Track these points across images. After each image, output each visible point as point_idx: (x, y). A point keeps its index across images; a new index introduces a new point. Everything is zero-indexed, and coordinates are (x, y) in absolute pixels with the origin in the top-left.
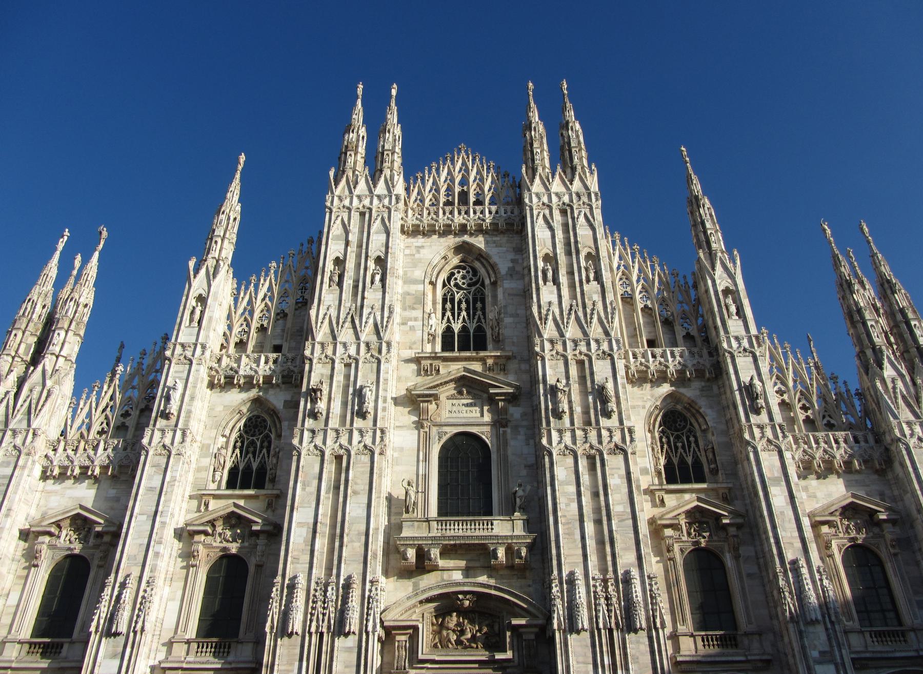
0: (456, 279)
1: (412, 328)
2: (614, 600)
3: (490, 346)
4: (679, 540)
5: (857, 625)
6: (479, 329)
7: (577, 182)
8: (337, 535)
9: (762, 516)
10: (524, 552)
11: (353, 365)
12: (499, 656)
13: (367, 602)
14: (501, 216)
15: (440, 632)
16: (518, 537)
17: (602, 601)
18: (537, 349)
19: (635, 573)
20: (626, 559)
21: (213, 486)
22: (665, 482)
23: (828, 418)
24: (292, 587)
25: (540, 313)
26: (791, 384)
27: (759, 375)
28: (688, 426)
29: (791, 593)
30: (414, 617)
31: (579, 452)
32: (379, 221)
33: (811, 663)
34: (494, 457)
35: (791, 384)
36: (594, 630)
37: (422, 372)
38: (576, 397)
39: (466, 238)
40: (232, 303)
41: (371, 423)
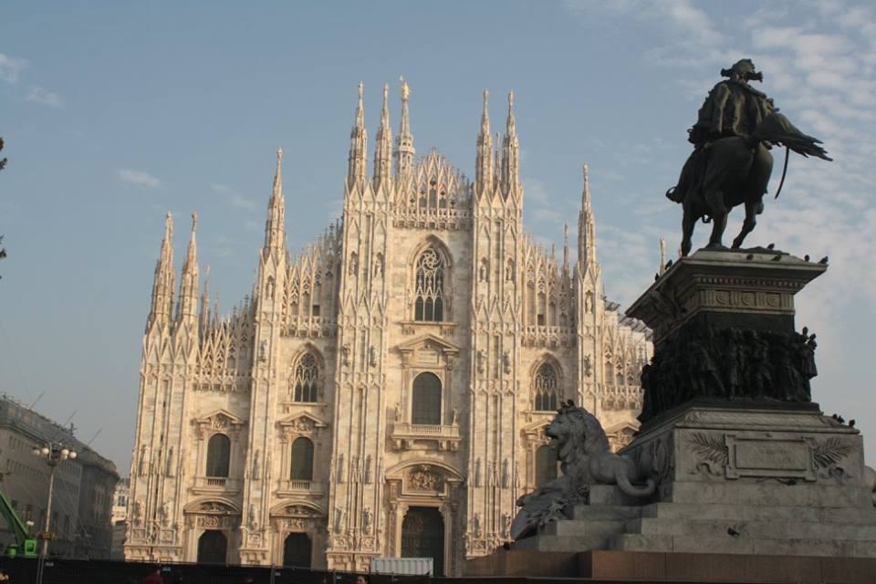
1: (398, 300)
2: (498, 473)
3: (445, 314)
7: (509, 200)
8: (362, 433)
10: (456, 445)
11: (367, 332)
12: (440, 495)
13: (378, 468)
18: (473, 328)
19: (510, 460)
20: (507, 452)
21: (288, 399)
24: (341, 460)
27: (595, 352)
30: (400, 476)
31: (489, 394)
32: (379, 225)
35: (615, 352)
36: (487, 486)
37: (405, 332)
38: (492, 359)
39: (434, 232)
41: (378, 370)
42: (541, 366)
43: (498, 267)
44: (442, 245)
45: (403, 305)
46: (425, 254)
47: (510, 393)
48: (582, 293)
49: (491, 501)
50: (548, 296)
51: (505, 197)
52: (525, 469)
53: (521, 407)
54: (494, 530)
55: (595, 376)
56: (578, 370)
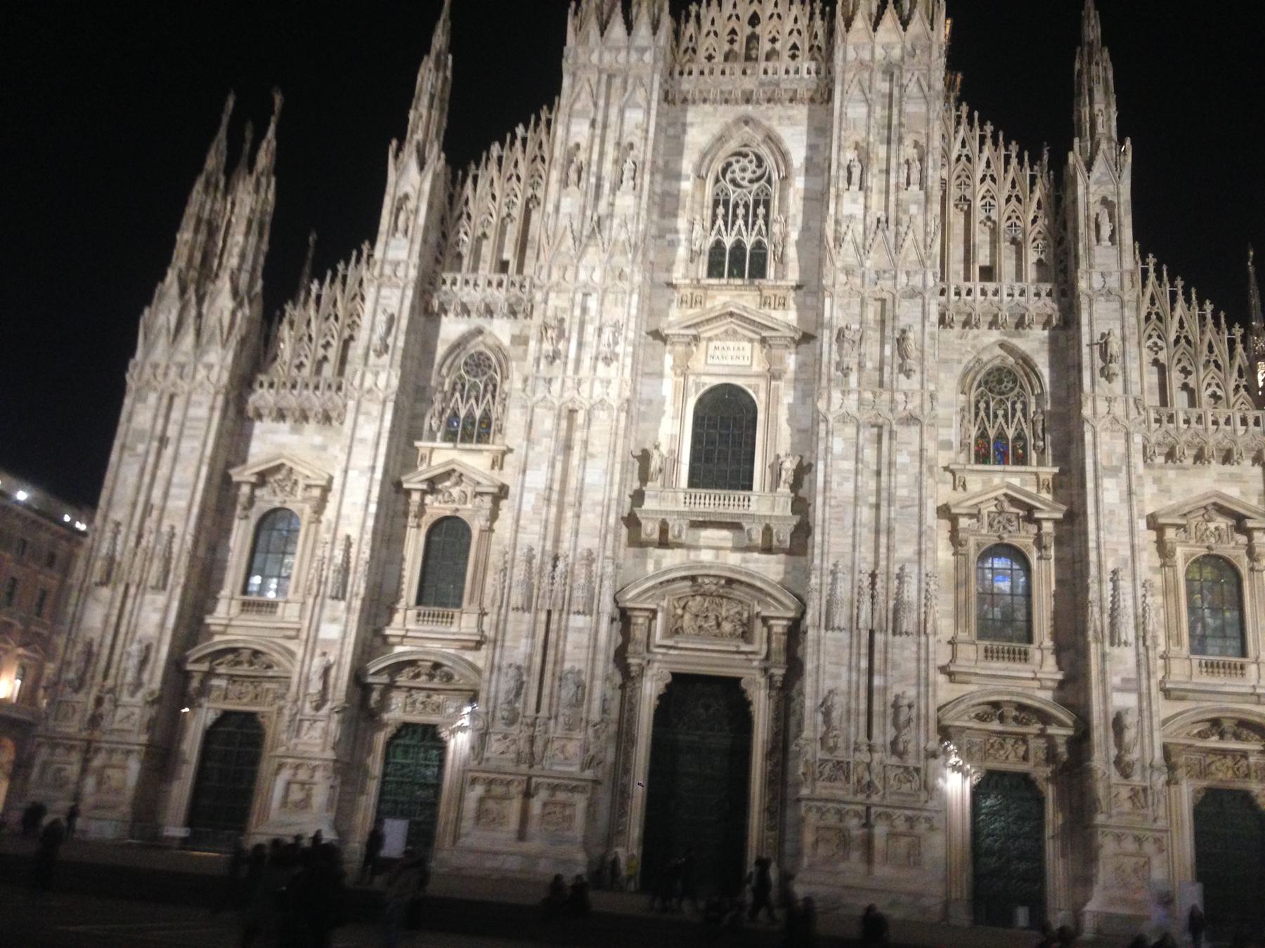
0: (733, 172)
2: (881, 598)
3: (771, 270)
4: (975, 533)
5: (1185, 650)
6: (759, 245)
7: (916, 26)
9: (1085, 513)
14: (802, 78)
15: (682, 616)
16: (777, 517)
17: (866, 599)
22: (973, 461)
23: (1214, 388)
25: (836, 231)
26: (1172, 337)
27: (1123, 327)
28: (1017, 389)
29: (1101, 608)
33: (1109, 690)
34: (761, 417)
40: (446, 201)
42: (989, 374)
43: (888, 160)
44: (771, 139)
45: (682, 252)
46: (733, 159)
47: (911, 420)
48: (1088, 204)
49: (864, 664)
50: (1004, 225)
51: (905, 23)
52: (952, 596)
53: (944, 458)
54: (869, 736)
55: (1125, 381)
56: (1080, 370)
